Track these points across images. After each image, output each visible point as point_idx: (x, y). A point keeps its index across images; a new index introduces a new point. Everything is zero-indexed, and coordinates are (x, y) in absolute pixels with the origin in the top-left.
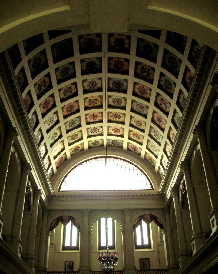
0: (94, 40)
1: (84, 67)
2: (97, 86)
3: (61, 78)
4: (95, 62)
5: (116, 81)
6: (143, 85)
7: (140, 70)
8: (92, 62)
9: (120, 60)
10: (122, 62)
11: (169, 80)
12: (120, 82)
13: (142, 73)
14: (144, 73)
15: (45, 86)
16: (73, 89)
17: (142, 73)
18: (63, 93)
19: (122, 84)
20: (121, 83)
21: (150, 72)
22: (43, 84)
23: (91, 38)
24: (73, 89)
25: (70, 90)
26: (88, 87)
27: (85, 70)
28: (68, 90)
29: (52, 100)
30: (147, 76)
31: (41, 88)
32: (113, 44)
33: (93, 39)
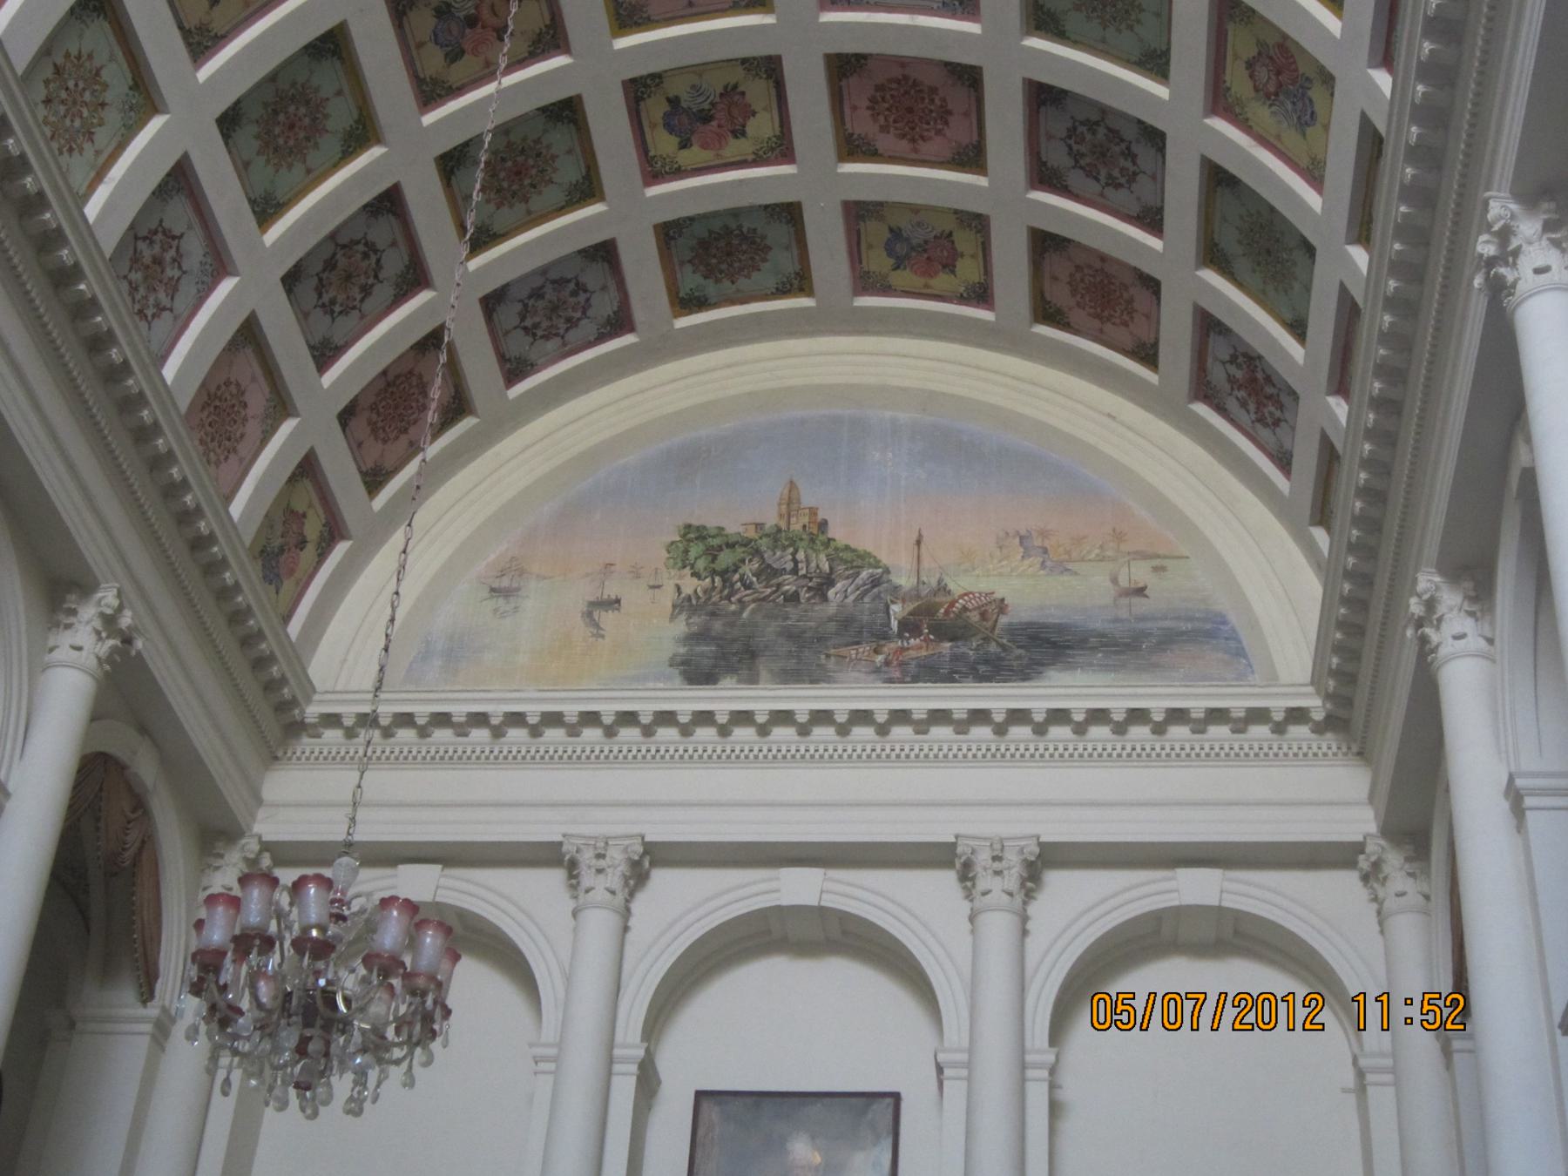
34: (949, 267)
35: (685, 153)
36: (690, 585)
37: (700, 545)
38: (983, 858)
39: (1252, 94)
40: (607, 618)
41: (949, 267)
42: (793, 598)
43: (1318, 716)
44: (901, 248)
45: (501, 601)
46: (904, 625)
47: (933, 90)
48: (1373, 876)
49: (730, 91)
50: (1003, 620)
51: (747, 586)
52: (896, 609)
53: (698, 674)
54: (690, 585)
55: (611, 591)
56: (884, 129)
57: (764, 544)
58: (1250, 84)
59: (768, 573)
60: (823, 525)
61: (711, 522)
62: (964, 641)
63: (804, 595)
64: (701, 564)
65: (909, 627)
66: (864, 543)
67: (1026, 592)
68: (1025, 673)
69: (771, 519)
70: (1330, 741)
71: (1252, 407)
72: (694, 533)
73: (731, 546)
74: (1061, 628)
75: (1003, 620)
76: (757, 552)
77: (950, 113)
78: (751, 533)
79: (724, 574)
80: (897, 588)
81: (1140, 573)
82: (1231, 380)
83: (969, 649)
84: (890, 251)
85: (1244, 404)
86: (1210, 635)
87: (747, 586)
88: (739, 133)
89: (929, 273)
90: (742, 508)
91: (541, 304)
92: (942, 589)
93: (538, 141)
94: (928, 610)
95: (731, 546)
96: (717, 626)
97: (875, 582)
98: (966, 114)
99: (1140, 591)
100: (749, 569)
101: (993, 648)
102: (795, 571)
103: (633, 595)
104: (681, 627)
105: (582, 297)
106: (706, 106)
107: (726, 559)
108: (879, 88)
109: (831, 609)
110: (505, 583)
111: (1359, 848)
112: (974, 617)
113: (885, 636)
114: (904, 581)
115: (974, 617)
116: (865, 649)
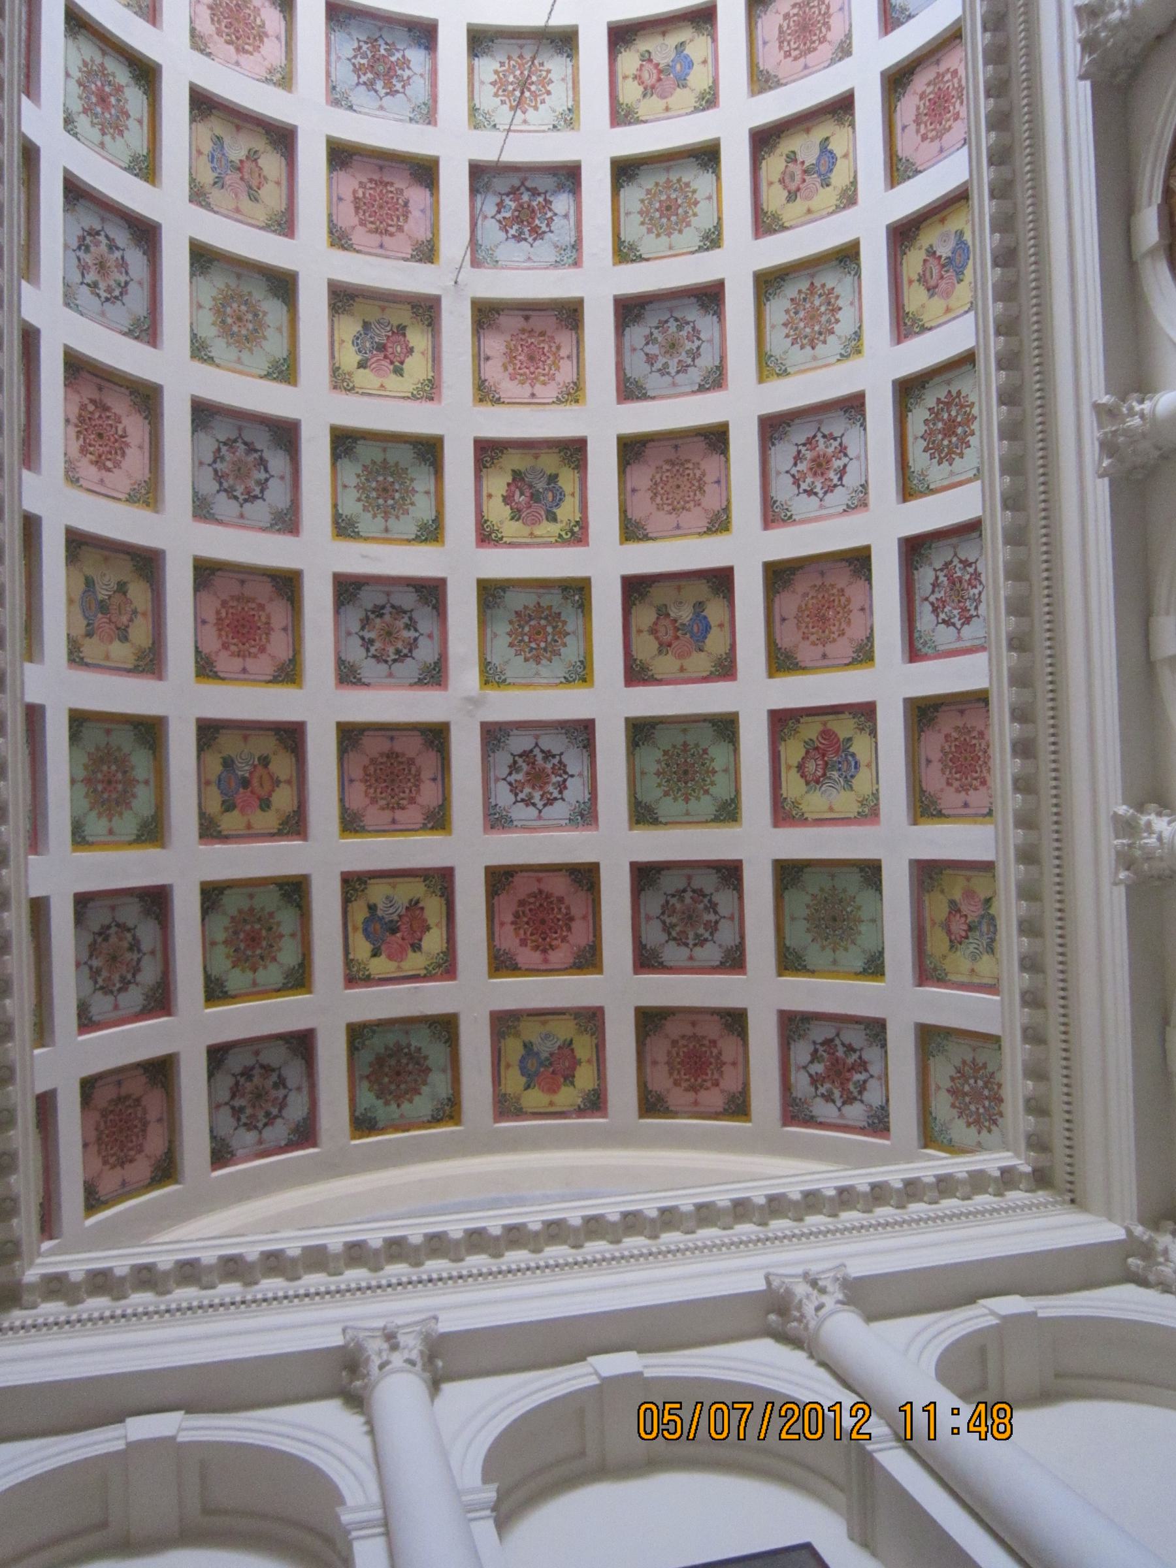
0: (510, 369)
1: (566, 216)
2: (497, 66)
3: (696, 176)
4: (503, 235)
5: (392, 93)
6: (237, 63)
7: (265, 178)
8: (519, 238)
9: (375, 239)
10: (362, 223)
11: (108, 138)
12: (370, 85)
13: (253, 156)
14: (242, 154)
15: (792, 158)
16: (635, 77)
17: (253, 156)
18: (691, 65)
19: (358, 70)
20: (363, 79)
21: (214, 169)
22: (798, 178)
23: (522, 383)
24: (635, 77)
25: (649, 76)
26: (549, 71)
27: (560, 188)
28: (659, 80)
29: (765, 43)
30: (227, 141)
31: (819, 159)
32: (418, 339)
33: (512, 378)
35: (375, 960)
39: (804, 788)
41: (569, 1078)
44: (532, 1064)
47: (561, 900)
49: (415, 905)
56: (523, 943)
58: (802, 781)
71: (837, 1093)
77: (572, 919)
82: (815, 1081)
84: (524, 1071)
85: (828, 1098)
88: (416, 947)
89: (553, 1090)
91: (249, 1086)
93: (271, 915)
98: (584, 918)
105: (281, 1093)
106: (395, 917)
108: (522, 903)
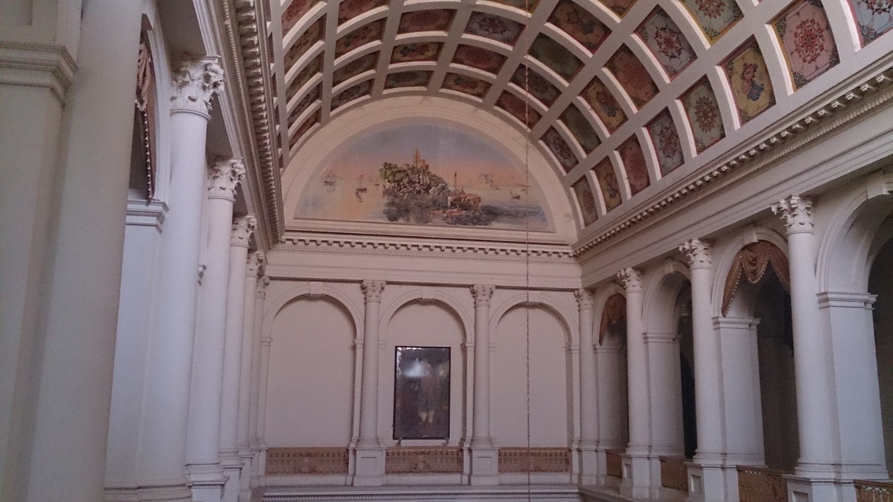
34: (473, 88)
36: (388, 185)
37: (390, 170)
38: (480, 291)
40: (363, 195)
42: (419, 192)
43: (571, 255)
45: (329, 187)
46: (452, 203)
48: (578, 296)
50: (480, 204)
51: (405, 187)
52: (449, 198)
53: (393, 219)
54: (388, 185)
55: (363, 186)
57: (409, 172)
59: (411, 182)
60: (427, 166)
61: (393, 163)
62: (472, 212)
63: (422, 191)
64: (391, 178)
65: (453, 205)
66: (439, 175)
67: (488, 196)
68: (486, 222)
69: (411, 164)
70: (572, 260)
72: (388, 166)
73: (400, 172)
74: (496, 208)
75: (480, 204)
76: (407, 175)
78: (405, 168)
79: (398, 182)
80: (449, 191)
81: (518, 191)
83: (470, 213)
86: (537, 213)
87: (405, 187)
90: (402, 160)
92: (462, 192)
94: (459, 199)
95: (400, 172)
96: (397, 201)
97: (443, 188)
99: (518, 197)
100: (406, 180)
101: (477, 214)
102: (419, 182)
103: (371, 188)
104: (386, 200)
107: (398, 176)
109: (430, 197)
110: (329, 180)
111: (578, 289)
112: (472, 203)
113: (446, 207)
114: (451, 189)
115: (472, 203)
116: (441, 211)
